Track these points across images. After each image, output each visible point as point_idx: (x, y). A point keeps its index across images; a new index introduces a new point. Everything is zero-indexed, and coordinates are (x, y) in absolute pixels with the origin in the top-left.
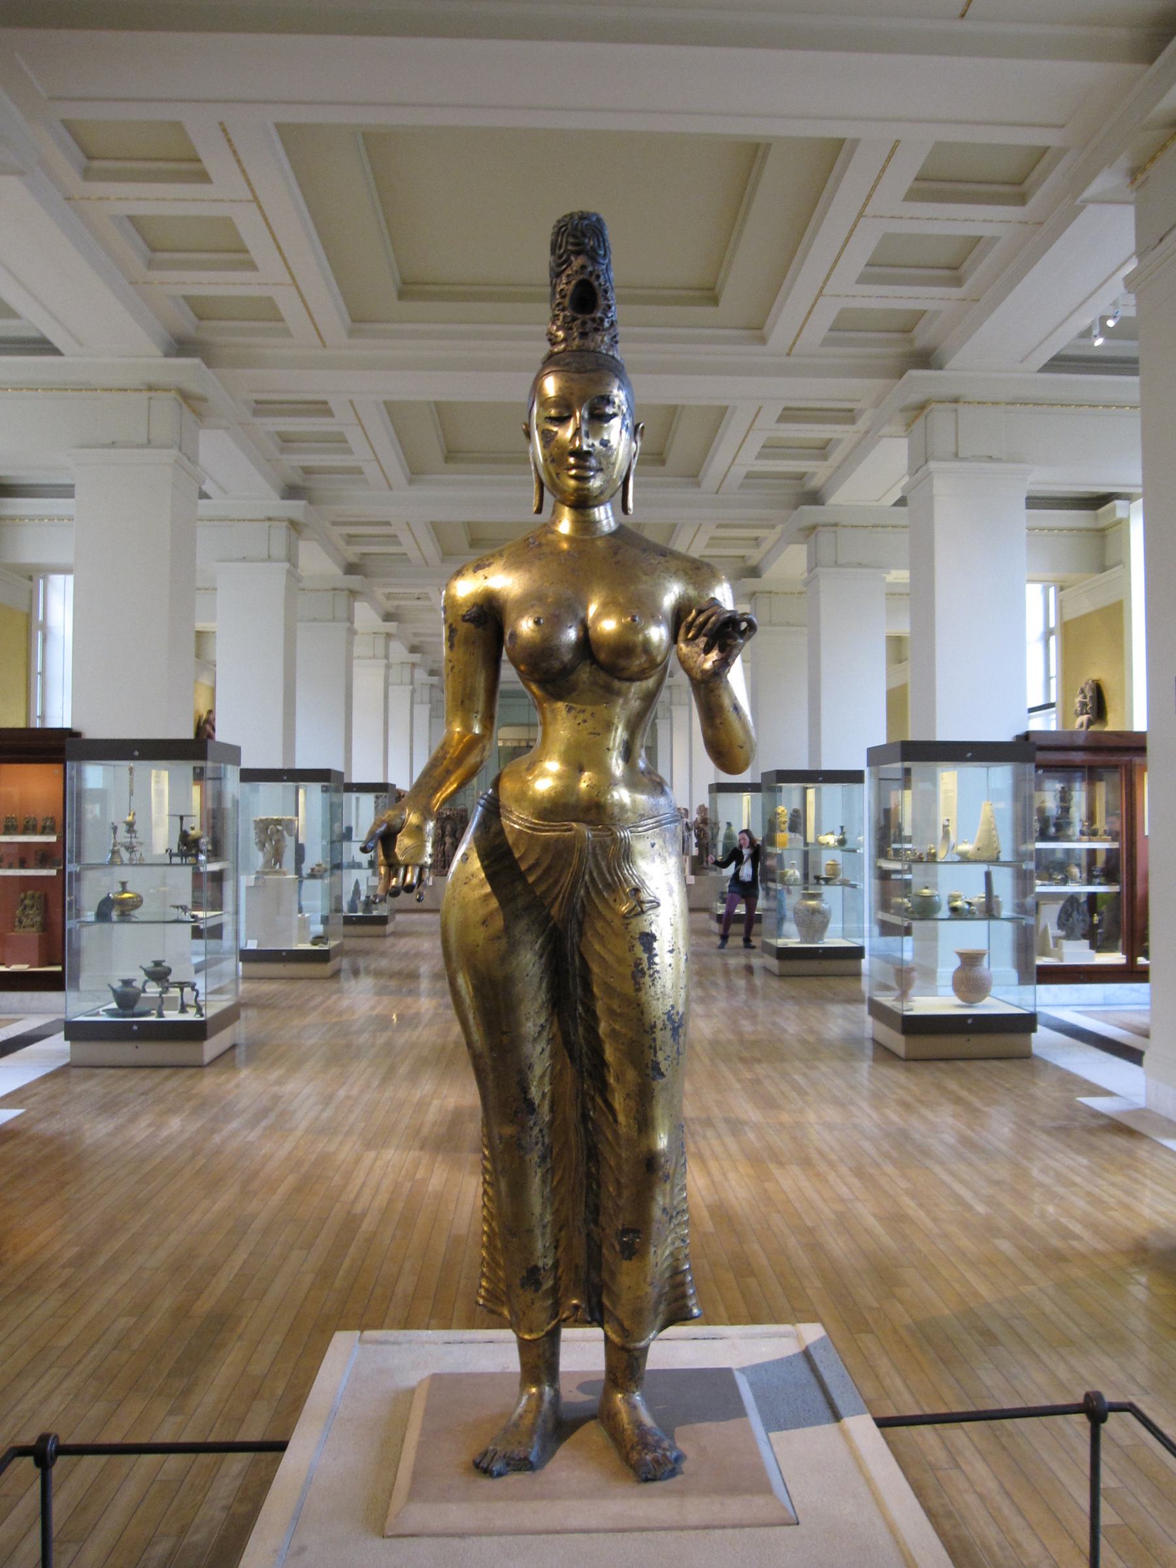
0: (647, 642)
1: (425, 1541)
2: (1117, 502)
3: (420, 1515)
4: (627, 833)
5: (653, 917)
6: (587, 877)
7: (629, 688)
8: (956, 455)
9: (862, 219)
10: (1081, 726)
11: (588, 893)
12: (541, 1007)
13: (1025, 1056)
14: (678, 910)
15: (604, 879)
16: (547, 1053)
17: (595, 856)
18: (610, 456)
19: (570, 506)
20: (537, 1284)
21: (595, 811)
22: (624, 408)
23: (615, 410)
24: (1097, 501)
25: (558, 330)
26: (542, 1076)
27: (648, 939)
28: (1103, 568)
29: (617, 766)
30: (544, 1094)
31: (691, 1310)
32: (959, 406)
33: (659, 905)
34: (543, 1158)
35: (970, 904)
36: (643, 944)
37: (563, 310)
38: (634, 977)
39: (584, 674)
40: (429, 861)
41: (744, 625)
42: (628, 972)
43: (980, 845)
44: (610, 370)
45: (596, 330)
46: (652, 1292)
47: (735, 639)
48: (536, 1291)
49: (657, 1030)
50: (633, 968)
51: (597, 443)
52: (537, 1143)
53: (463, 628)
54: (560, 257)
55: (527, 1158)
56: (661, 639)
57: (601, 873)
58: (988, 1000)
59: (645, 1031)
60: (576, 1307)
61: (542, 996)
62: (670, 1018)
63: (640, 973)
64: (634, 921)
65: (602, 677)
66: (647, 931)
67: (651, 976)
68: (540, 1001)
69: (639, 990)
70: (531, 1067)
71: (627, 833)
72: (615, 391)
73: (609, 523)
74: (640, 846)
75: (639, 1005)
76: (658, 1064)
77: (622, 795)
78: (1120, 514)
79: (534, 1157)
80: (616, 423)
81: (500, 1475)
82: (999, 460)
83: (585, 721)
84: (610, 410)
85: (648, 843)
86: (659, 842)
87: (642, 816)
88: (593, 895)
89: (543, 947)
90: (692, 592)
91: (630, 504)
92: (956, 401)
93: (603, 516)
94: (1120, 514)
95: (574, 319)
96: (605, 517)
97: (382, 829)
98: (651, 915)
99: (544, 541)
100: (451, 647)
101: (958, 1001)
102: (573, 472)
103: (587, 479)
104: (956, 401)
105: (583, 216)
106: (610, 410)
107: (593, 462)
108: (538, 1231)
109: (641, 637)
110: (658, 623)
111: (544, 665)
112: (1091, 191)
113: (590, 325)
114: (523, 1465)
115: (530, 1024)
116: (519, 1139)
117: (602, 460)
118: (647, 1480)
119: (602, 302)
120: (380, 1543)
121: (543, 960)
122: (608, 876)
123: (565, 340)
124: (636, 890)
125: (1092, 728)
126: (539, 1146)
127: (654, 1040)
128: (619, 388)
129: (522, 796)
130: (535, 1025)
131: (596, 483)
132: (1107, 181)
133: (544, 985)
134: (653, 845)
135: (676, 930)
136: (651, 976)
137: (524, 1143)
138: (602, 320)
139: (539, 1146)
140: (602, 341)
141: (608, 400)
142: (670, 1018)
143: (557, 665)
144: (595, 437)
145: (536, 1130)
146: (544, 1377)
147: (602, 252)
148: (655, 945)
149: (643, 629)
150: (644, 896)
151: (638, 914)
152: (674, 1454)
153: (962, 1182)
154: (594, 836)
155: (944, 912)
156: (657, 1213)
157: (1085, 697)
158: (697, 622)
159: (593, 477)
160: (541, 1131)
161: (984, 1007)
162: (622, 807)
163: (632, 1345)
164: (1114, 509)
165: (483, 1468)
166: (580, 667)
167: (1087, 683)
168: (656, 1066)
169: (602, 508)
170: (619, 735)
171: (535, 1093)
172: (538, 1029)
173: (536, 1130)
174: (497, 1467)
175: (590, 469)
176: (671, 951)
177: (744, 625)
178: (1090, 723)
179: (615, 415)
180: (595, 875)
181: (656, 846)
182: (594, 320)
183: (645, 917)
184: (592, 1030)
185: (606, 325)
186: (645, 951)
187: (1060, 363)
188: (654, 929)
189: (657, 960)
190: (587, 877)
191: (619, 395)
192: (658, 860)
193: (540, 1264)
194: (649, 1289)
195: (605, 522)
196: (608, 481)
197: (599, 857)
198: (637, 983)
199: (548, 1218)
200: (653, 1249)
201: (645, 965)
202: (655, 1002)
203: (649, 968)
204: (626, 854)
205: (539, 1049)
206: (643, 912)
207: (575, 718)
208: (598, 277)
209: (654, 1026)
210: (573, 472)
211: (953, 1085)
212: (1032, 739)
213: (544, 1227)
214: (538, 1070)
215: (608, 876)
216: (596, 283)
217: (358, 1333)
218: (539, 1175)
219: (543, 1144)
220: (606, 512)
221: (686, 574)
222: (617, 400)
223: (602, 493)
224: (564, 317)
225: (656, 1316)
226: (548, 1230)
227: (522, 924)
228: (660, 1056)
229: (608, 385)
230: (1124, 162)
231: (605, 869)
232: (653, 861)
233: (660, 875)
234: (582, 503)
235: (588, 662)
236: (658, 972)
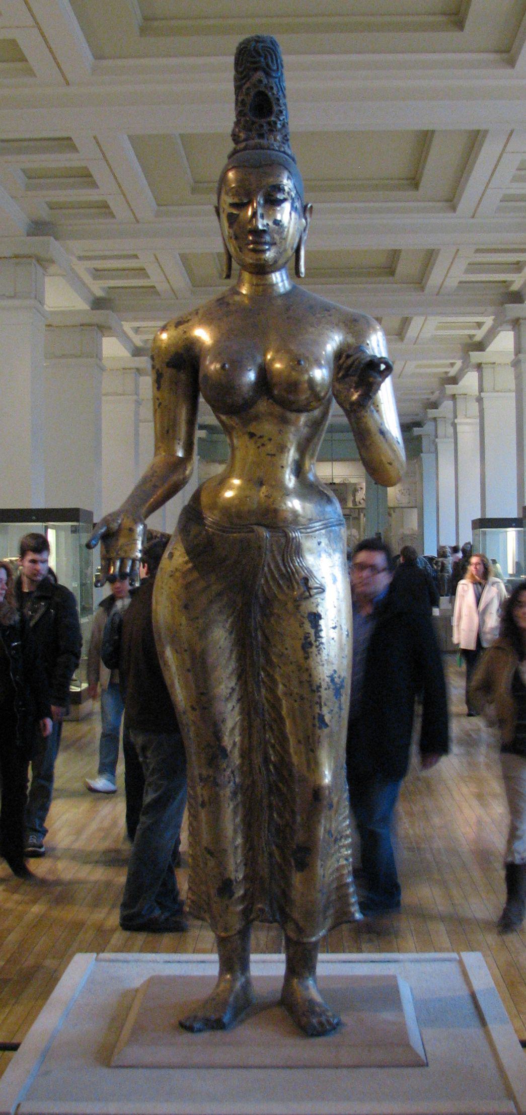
0: (311, 381)
1: (140, 1070)
3: (134, 1053)
4: (297, 534)
5: (319, 600)
6: (266, 569)
7: (298, 418)
12: (232, 674)
14: (342, 595)
15: (279, 570)
16: (237, 709)
17: (272, 551)
18: (282, 232)
19: (250, 273)
20: (231, 894)
21: (272, 518)
22: (293, 194)
23: (286, 196)
25: (240, 131)
26: (233, 729)
27: (315, 618)
29: (290, 481)
30: (235, 744)
31: (353, 914)
33: (324, 591)
34: (235, 794)
36: (311, 621)
39: (263, 406)
40: (139, 555)
41: (383, 367)
42: (298, 644)
44: (280, 164)
45: (271, 131)
46: (320, 898)
47: (375, 378)
48: (231, 897)
49: (322, 690)
51: (271, 223)
52: (229, 782)
53: (168, 373)
54: (242, 73)
55: (222, 793)
56: (323, 379)
57: (277, 566)
59: (313, 691)
60: (262, 910)
61: (233, 665)
62: (332, 680)
63: (309, 643)
64: (304, 603)
65: (278, 409)
66: (315, 611)
67: (317, 647)
68: (230, 668)
69: (307, 658)
70: (224, 721)
71: (297, 534)
72: (285, 181)
73: (284, 285)
74: (308, 544)
75: (307, 670)
76: (323, 716)
77: (295, 504)
79: (228, 791)
80: (287, 206)
81: (200, 1030)
83: (263, 445)
84: (280, 196)
85: (315, 541)
86: (324, 542)
87: (310, 520)
89: (233, 625)
90: (351, 340)
91: (303, 269)
93: (279, 280)
95: (253, 123)
96: (280, 280)
97: (103, 530)
98: (318, 598)
99: (231, 301)
103: (264, 251)
105: (258, 40)
106: (280, 196)
107: (267, 238)
108: (230, 851)
109: (306, 377)
110: (320, 366)
111: (229, 401)
113: (266, 128)
114: (217, 1025)
115: (222, 686)
116: (215, 778)
117: (276, 236)
118: (312, 1035)
119: (275, 108)
120: (105, 1071)
121: (233, 636)
122: (283, 568)
123: (246, 140)
124: (306, 580)
126: (232, 783)
127: (320, 697)
128: (288, 178)
129: (214, 506)
130: (227, 688)
131: (270, 255)
133: (234, 656)
134: (319, 543)
135: (339, 611)
136: (317, 647)
137: (219, 781)
138: (275, 123)
139: (232, 783)
140: (275, 140)
141: (279, 188)
142: (332, 680)
143: (241, 401)
144: (269, 218)
145: (228, 772)
146: (237, 967)
147: (275, 68)
148: (322, 622)
149: (307, 371)
150: (311, 583)
152: (336, 1021)
154: (271, 537)
156: (321, 832)
158: (345, 365)
159: (268, 250)
160: (233, 772)
162: (294, 513)
163: (305, 940)
165: (186, 1027)
166: (259, 402)
168: (321, 718)
169: (278, 274)
170: (292, 454)
171: (227, 742)
172: (229, 691)
173: (228, 772)
174: (197, 1025)
175: (265, 243)
176: (334, 628)
177: (383, 367)
179: (285, 200)
180: (272, 566)
181: (323, 545)
182: (269, 123)
183: (312, 600)
184: (272, 690)
185: (279, 126)
186: (312, 627)
188: (320, 610)
189: (323, 634)
190: (266, 569)
191: (287, 183)
192: (324, 555)
193: (233, 877)
194: (319, 895)
195: (280, 285)
196: (280, 253)
197: (276, 552)
198: (306, 652)
199: (239, 841)
200: (319, 863)
201: (313, 638)
202: (320, 667)
203: (316, 641)
204: (298, 551)
205: (230, 706)
206: (311, 596)
207: (256, 443)
208: (272, 88)
209: (320, 687)
213: (236, 848)
214: (230, 724)
215: (283, 568)
216: (270, 94)
217: (95, 955)
218: (232, 806)
219: (235, 783)
220: (282, 277)
221: (346, 325)
222: (286, 188)
223: (276, 262)
224: (246, 121)
225: (325, 918)
226: (239, 850)
227: (216, 607)
228: (325, 710)
229: (279, 176)
231: (280, 562)
232: (320, 556)
233: (328, 572)
234: (262, 270)
235: (266, 398)
236: (322, 643)
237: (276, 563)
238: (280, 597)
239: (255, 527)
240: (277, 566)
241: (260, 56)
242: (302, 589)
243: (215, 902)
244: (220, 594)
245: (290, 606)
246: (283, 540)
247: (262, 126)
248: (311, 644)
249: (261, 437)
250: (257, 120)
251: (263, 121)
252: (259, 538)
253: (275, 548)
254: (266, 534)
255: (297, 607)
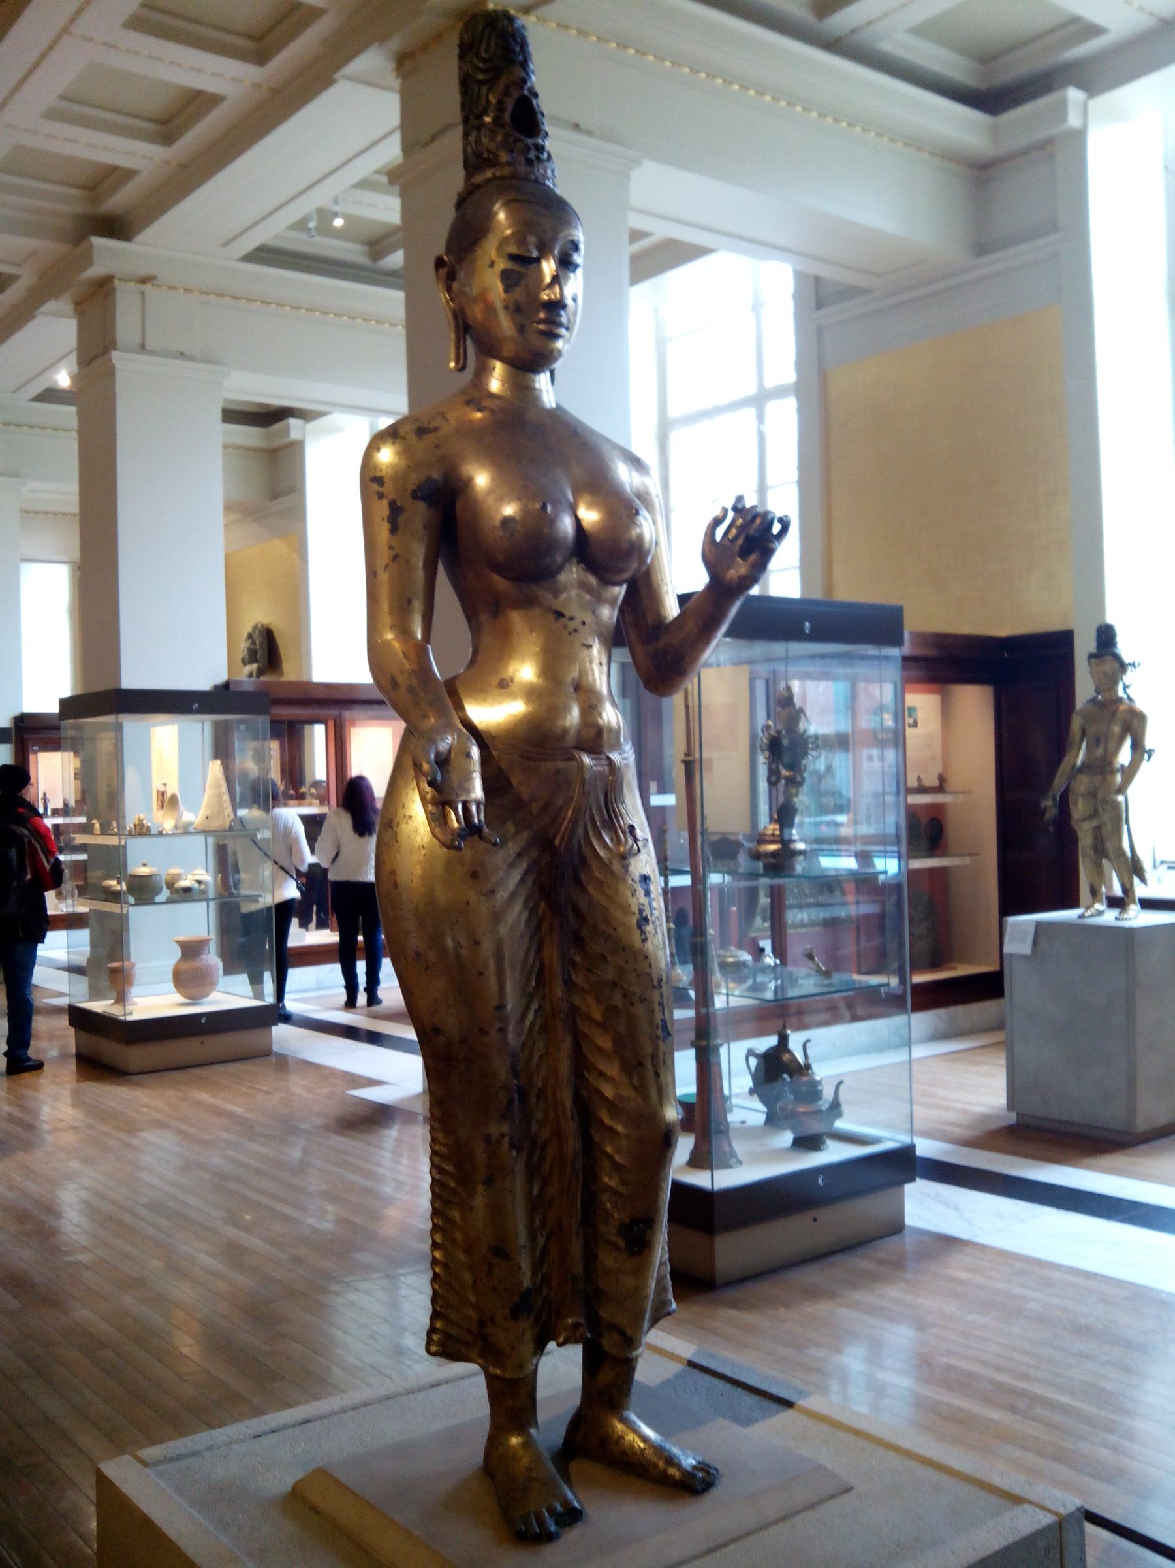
2: (293, 422)
8: (143, 346)
9: (66, 38)
10: (250, 675)
11: (586, 832)
13: (265, 1053)
24: (269, 417)
28: (275, 495)
32: (148, 287)
35: (199, 882)
37: (502, 126)
38: (639, 927)
42: (634, 920)
43: (208, 813)
50: (638, 915)
58: (214, 995)
59: (654, 987)
69: (645, 940)
75: (646, 957)
78: (294, 435)
82: (191, 358)
83: (576, 631)
88: (591, 834)
92: (144, 280)
94: (294, 435)
95: (517, 140)
100: (394, 530)
101: (180, 998)
102: (541, 327)
103: (558, 337)
104: (144, 280)
112: (352, 68)
113: (532, 154)
123: (509, 164)
125: (263, 679)
127: (662, 995)
132: (374, 61)
151: (635, 854)
153: (278, 1199)
155: (165, 894)
157: (253, 643)
161: (211, 1003)
164: (287, 430)
166: (567, 566)
167: (255, 628)
178: (260, 672)
187: (266, 255)
198: (643, 932)
201: (647, 912)
209: (660, 980)
210: (541, 327)
211: (204, 1096)
212: (232, 688)
216: (534, 102)
224: (507, 135)
230: (395, 43)
237: (598, 803)
238: (602, 853)
239: (576, 753)
240: (600, 810)
241: (516, 42)
242: (630, 840)
243: (505, 1330)
244: (519, 855)
245: (616, 866)
246: (606, 769)
247: (528, 149)
248: (646, 920)
249: (572, 619)
250: (522, 137)
251: (530, 141)
252: (581, 765)
253: (598, 783)
254: (587, 760)
255: (626, 868)
